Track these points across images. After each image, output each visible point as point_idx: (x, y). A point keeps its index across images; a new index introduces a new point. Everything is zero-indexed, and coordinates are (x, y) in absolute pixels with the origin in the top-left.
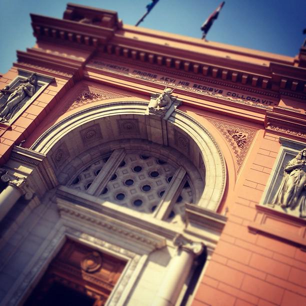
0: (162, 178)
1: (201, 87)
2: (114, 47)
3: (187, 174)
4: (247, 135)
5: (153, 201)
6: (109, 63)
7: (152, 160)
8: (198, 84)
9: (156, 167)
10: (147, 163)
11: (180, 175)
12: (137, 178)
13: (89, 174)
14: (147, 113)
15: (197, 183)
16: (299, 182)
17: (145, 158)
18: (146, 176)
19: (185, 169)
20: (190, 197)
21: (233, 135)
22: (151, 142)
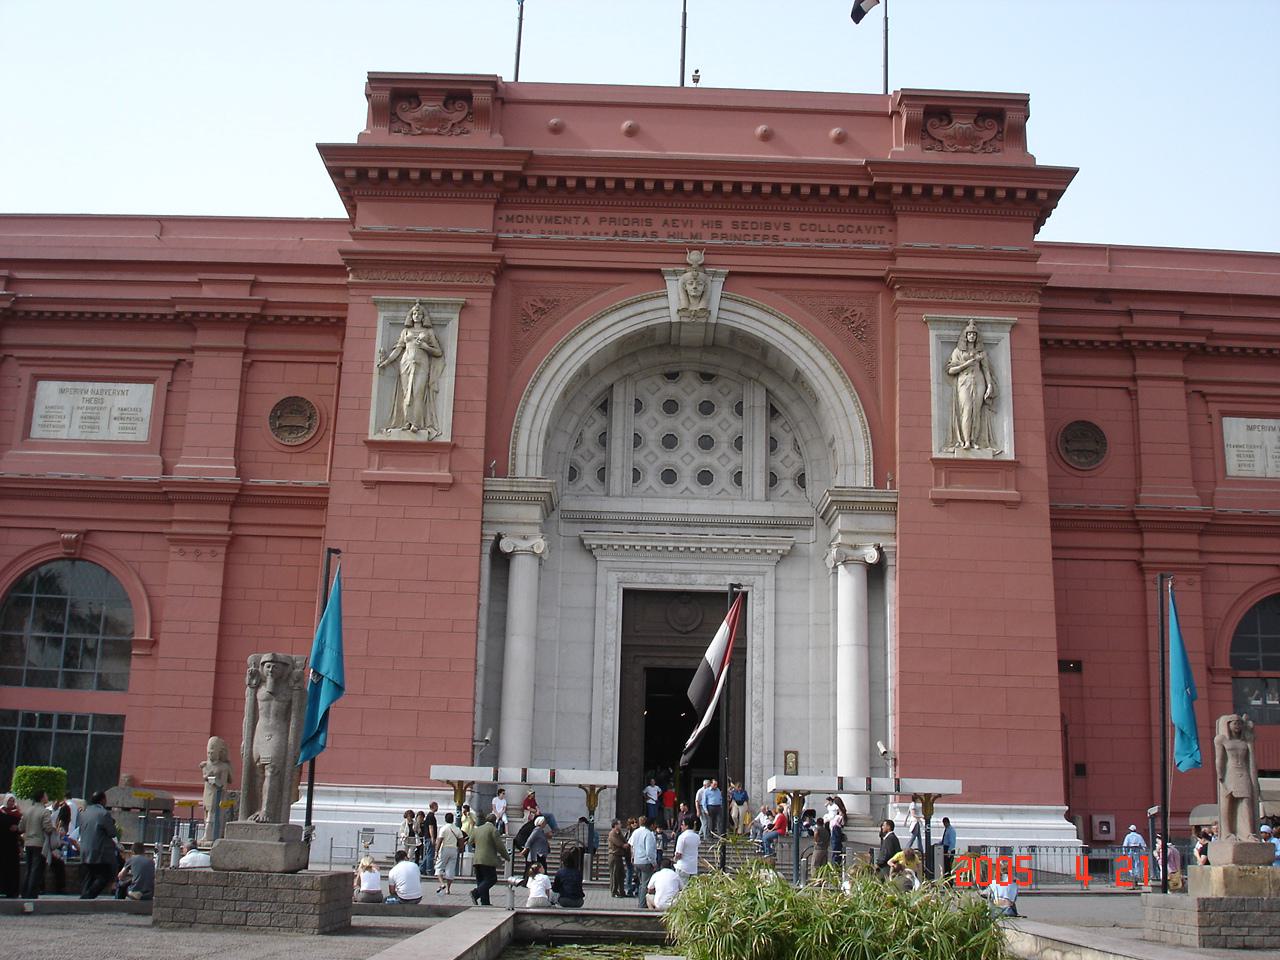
0: (724, 412)
1: (747, 225)
2: (542, 180)
3: (767, 390)
4: (863, 310)
5: (731, 466)
6: (539, 213)
7: (689, 380)
8: (739, 219)
9: (705, 391)
10: (683, 389)
11: (756, 401)
12: (682, 429)
13: (588, 451)
14: (675, 318)
15: (797, 410)
16: (976, 394)
17: (672, 376)
18: (696, 418)
19: (762, 384)
20: (790, 435)
21: (841, 319)
22: (677, 347)
